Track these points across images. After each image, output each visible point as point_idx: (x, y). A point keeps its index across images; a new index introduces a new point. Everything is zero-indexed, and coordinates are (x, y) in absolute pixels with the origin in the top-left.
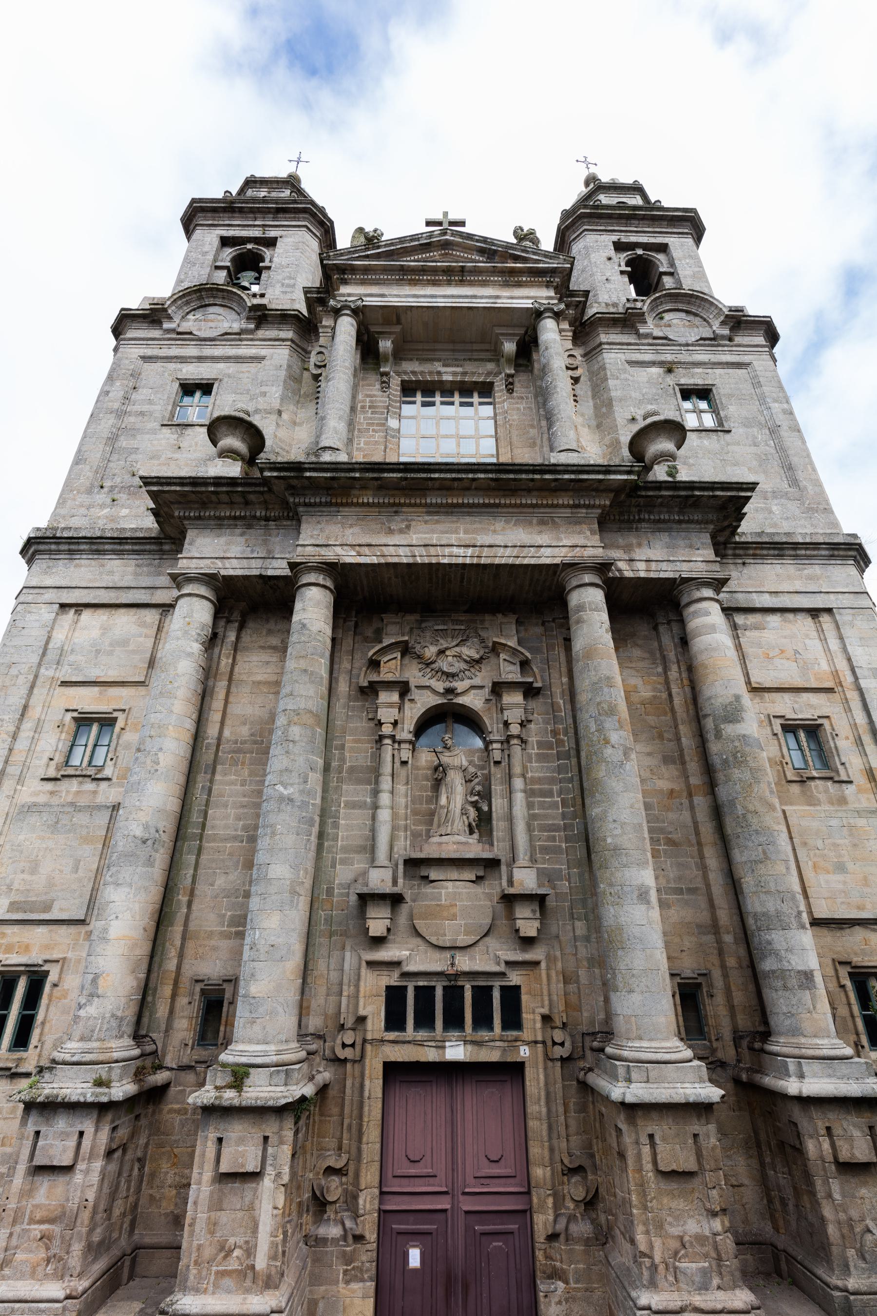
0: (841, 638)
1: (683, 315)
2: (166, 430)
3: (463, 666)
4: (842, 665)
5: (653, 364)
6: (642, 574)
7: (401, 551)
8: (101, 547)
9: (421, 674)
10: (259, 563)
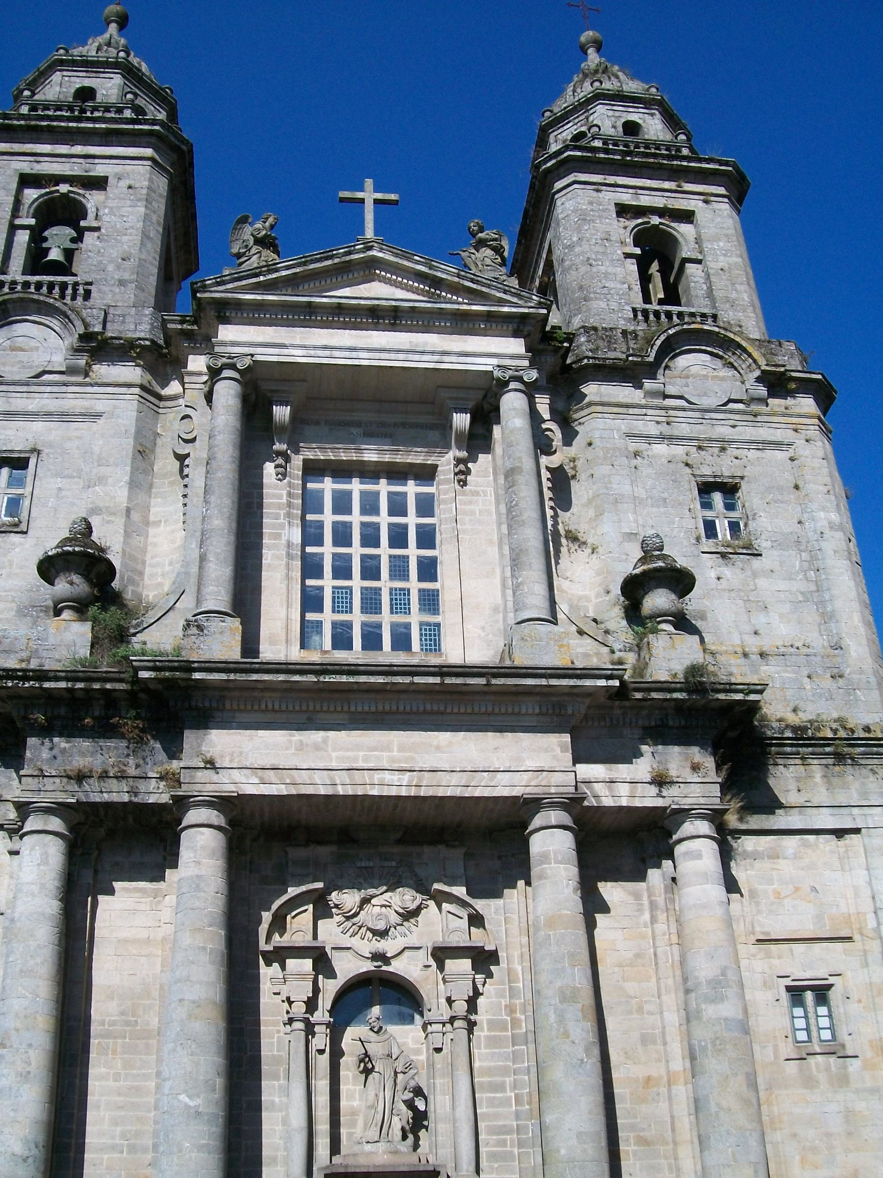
3: (395, 919)
7: (318, 777)
9: (341, 929)
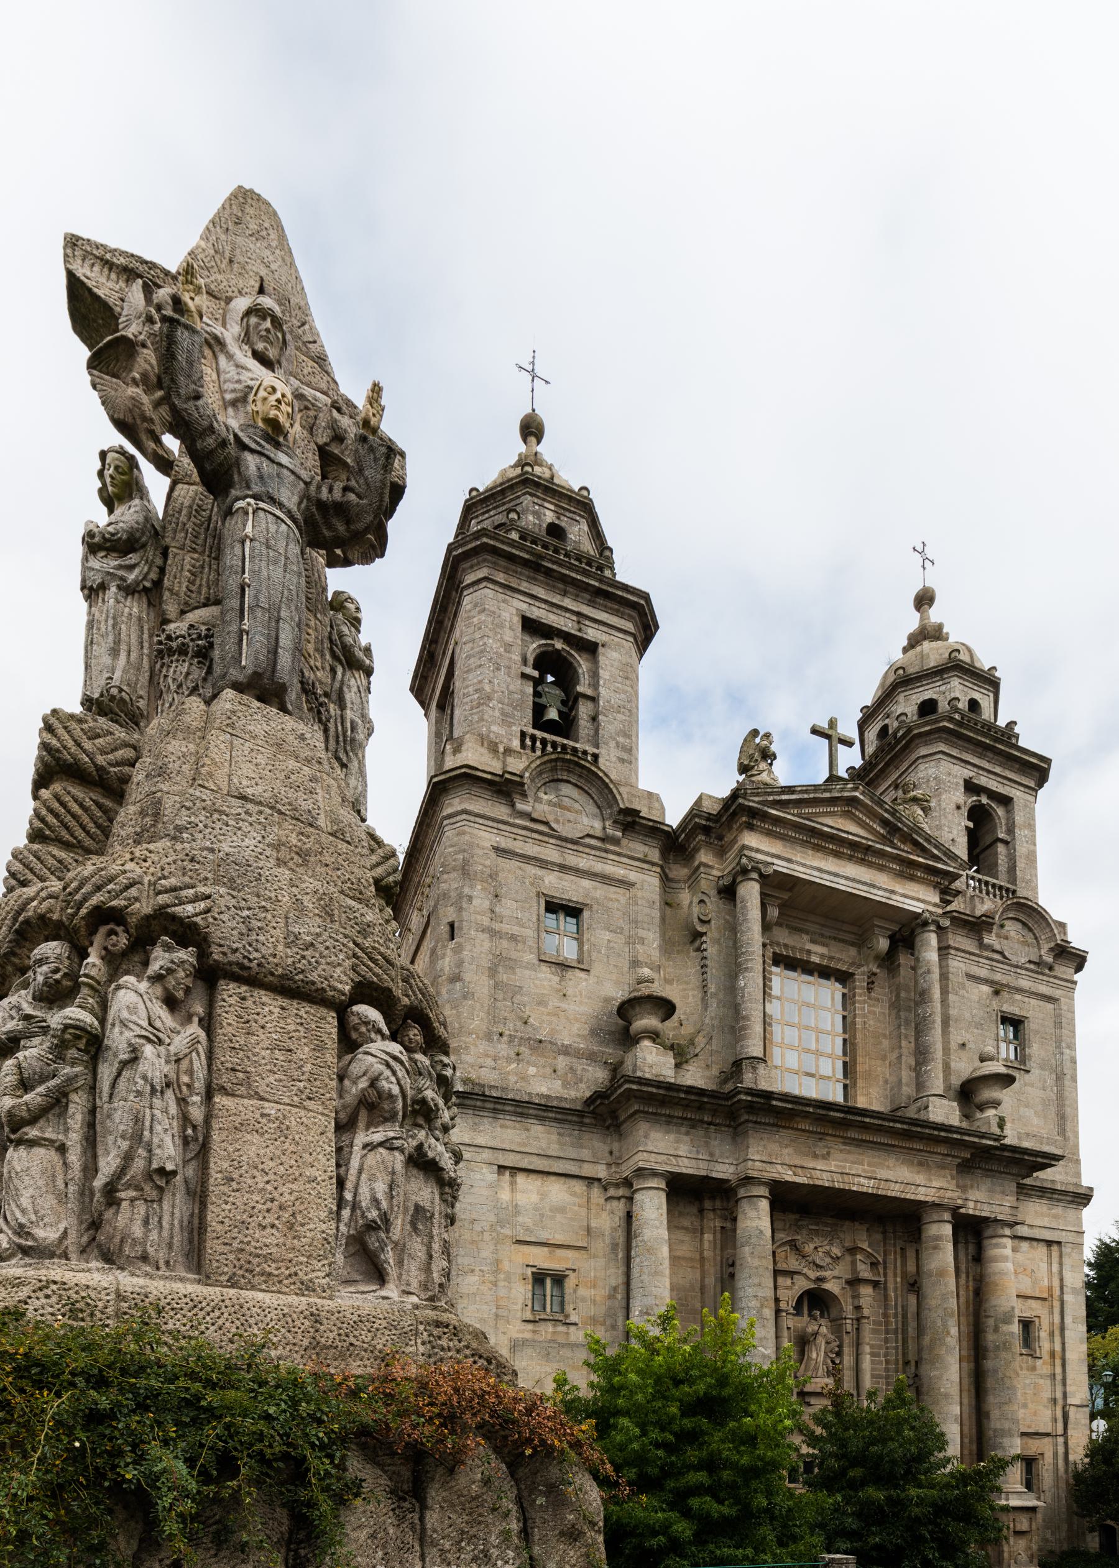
0: (1061, 1264)
1: (1019, 926)
2: (544, 968)
4: (1056, 1283)
5: (986, 981)
6: (971, 1212)
8: (525, 1111)
10: (702, 1165)
